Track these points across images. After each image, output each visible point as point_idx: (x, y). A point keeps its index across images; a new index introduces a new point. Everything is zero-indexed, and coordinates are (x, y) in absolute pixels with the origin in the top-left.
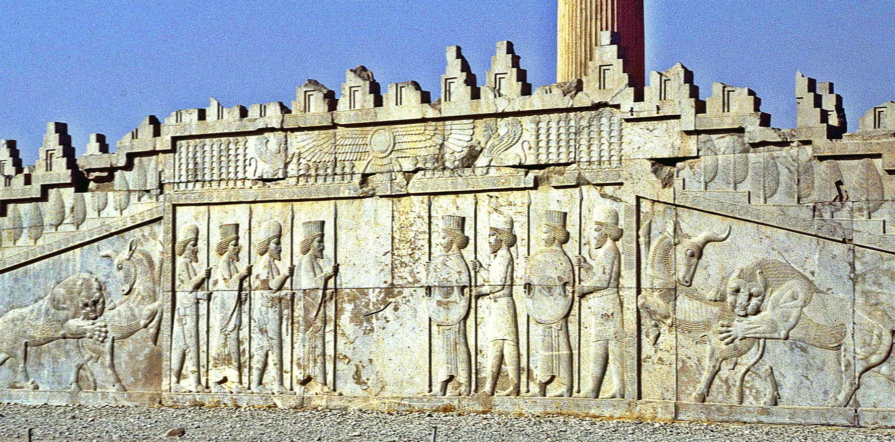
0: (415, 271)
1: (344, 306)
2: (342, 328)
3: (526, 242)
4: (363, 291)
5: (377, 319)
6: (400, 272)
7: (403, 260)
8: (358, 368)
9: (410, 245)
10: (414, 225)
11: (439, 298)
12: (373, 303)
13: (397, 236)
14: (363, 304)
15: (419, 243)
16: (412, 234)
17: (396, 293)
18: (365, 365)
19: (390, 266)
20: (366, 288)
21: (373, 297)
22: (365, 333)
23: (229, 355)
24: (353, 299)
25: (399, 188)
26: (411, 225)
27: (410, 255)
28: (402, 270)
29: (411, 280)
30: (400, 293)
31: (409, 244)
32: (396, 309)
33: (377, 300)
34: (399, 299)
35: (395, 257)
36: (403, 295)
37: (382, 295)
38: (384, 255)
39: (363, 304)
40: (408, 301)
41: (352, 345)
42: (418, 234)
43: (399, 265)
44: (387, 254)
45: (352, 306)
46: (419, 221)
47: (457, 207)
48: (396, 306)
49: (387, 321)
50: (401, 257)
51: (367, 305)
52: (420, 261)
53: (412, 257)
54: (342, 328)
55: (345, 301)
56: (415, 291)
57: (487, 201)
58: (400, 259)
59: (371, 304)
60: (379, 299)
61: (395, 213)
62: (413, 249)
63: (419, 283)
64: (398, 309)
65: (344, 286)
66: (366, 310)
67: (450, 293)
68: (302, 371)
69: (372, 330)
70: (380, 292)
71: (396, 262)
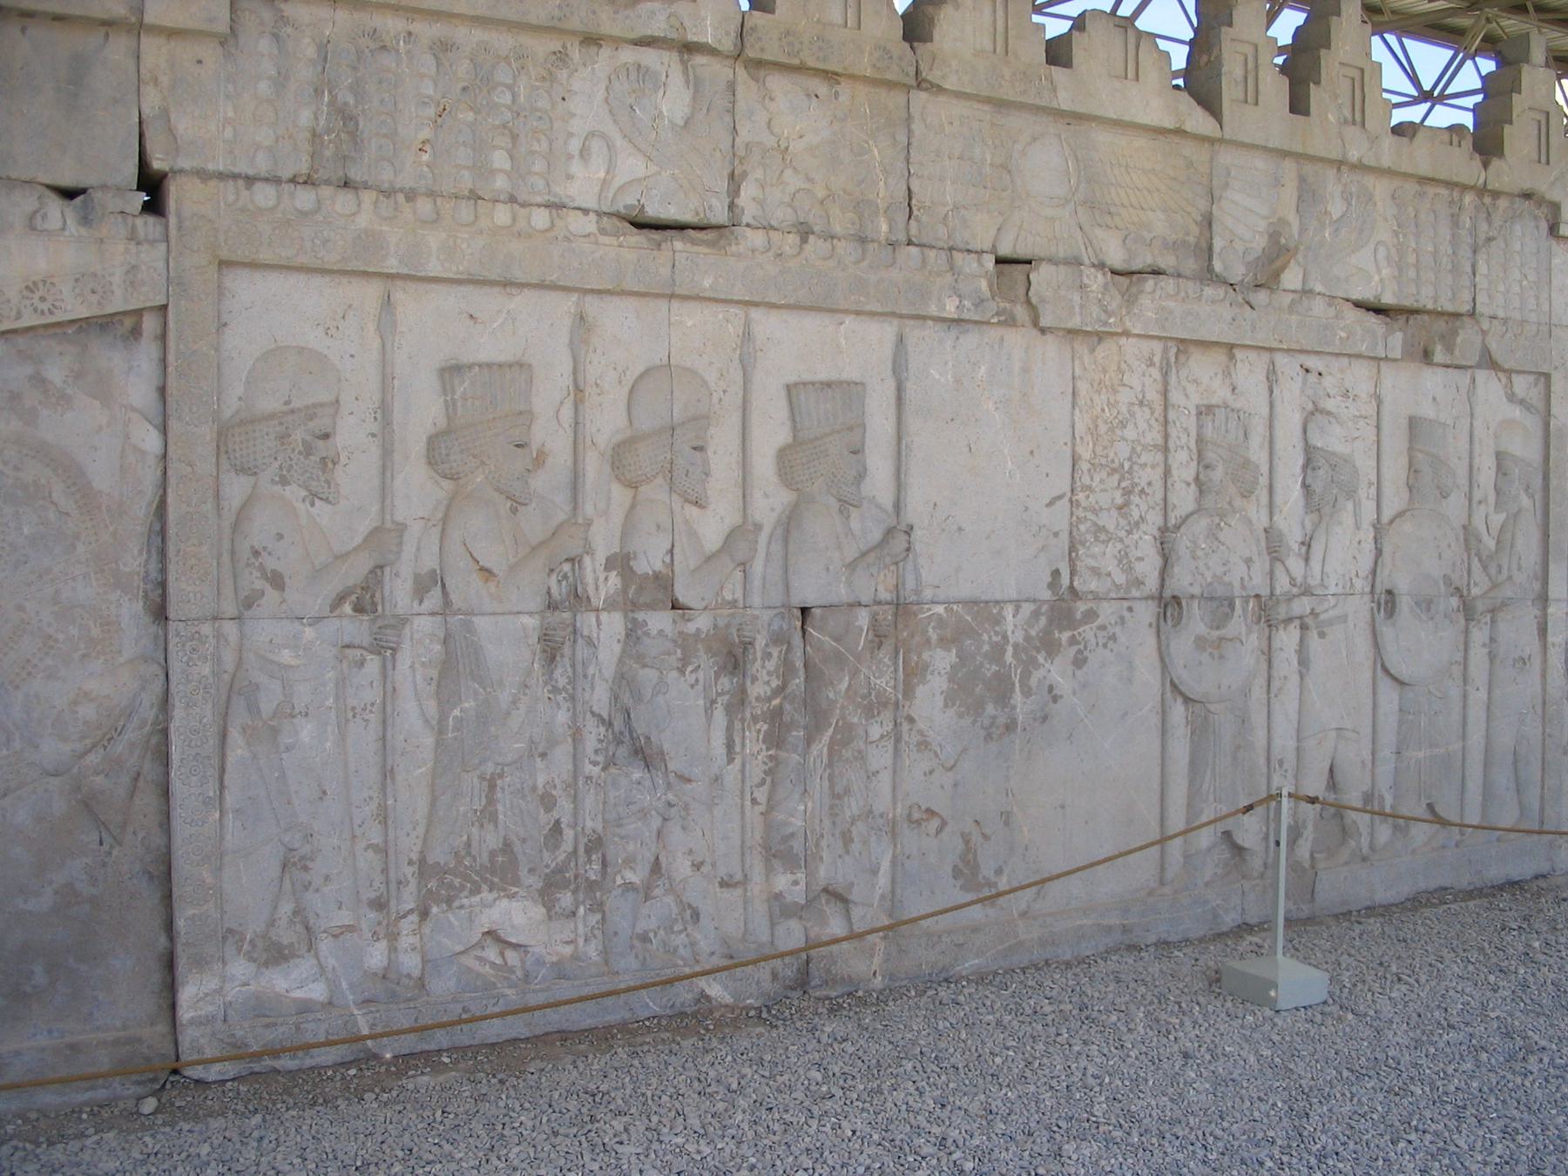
0: (1134, 554)
1: (926, 656)
2: (921, 725)
3: (1373, 490)
4: (985, 609)
5: (1027, 693)
6: (1094, 556)
7: (1101, 523)
8: (967, 842)
9: (1120, 482)
10: (1130, 426)
13: (1085, 452)
14: (986, 648)
15: (1144, 476)
16: (1123, 451)
17: (1078, 616)
18: (988, 831)
19: (1065, 537)
20: (997, 602)
21: (1013, 625)
22: (988, 737)
23: (507, 847)
24: (954, 637)
25: (1103, 317)
26: (1123, 425)
27: (1120, 508)
28: (1097, 549)
29: (1120, 578)
30: (1091, 615)
31: (1117, 476)
32: (1079, 662)
33: (1028, 638)
34: (1087, 631)
35: (1080, 513)
36: (1099, 622)
37: (1043, 621)
38: (1047, 505)
39: (986, 648)
40: (1113, 638)
41: (950, 774)
42: (1139, 449)
43: (1090, 538)
44: (1059, 504)
46: (1142, 415)
48: (1080, 652)
49: (1055, 699)
50: (1095, 512)
51: (998, 651)
52: (1143, 527)
53: (1125, 516)
54: (921, 725)
55: (928, 641)
56: (1130, 609)
57: (1299, 380)
58: (1092, 517)
59: (1010, 650)
60: (1033, 633)
61: (1083, 387)
62: (1127, 492)
64: (1085, 660)
65: (928, 594)
66: (994, 668)
67: (1227, 614)
68: (801, 876)
69: (1010, 727)
70: (1036, 614)
71: (1082, 528)
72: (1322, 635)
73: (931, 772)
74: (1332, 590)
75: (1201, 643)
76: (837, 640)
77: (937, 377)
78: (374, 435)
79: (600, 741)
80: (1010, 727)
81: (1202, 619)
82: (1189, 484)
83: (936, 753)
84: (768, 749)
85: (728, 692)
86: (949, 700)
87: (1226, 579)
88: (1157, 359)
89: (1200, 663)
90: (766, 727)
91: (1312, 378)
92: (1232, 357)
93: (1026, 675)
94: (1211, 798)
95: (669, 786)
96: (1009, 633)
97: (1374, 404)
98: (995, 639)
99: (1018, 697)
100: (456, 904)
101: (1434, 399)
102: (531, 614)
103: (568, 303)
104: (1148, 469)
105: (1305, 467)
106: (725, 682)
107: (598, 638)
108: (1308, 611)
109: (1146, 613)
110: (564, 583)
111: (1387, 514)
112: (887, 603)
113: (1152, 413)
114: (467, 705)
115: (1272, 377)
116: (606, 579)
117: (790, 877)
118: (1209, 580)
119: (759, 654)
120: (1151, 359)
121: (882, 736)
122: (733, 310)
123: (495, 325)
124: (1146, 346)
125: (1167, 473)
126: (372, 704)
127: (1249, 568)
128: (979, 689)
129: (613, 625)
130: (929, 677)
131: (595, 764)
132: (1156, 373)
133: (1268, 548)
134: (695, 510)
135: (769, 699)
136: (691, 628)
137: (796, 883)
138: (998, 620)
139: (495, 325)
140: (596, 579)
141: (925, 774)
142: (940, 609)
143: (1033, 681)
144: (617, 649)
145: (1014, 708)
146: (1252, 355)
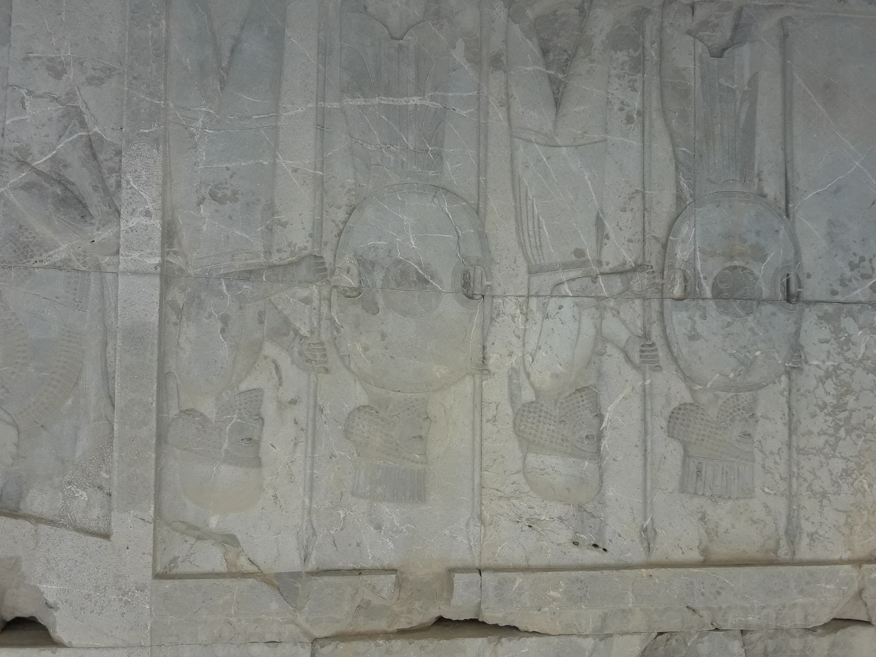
3: (489, 414)
11: (759, 270)
47: (703, 518)
52: (821, 373)
57: (608, 535)
63: (821, 314)
67: (722, 282)
72: (579, 253)
74: (568, 303)
75: (759, 254)
81: (756, 279)
82: (762, 416)
87: (728, 319)
88: (805, 541)
89: (758, 233)
91: (586, 537)
92: (704, 551)
94: (739, 95)
97: (487, 515)
101: (378, 527)
104: (815, 430)
105: (600, 437)
108: (600, 278)
109: (813, 289)
111: (467, 386)
113: (810, 486)
115: (648, 535)
118: (750, 318)
120: (812, 540)
124: (820, 553)
125: (791, 431)
127: (693, 329)
132: (807, 527)
133: (656, 350)
146: (677, 556)
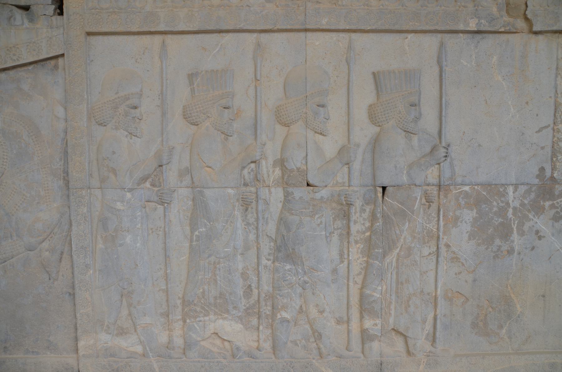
5: (522, 233)
12: (515, 209)
22: (496, 257)
23: (221, 295)
33: (523, 205)
39: (495, 209)
45: (474, 213)
51: (502, 212)
54: (454, 249)
59: (511, 211)
60: (526, 202)
65: (459, 180)
66: (500, 220)
69: (510, 252)
73: (460, 273)
76: (402, 204)
77: (465, 64)
78: (158, 106)
79: (270, 249)
80: (510, 252)
83: (462, 263)
84: (363, 257)
85: (340, 228)
86: (472, 236)
90: (362, 246)
93: (521, 225)
95: (305, 273)
96: (510, 202)
98: (501, 204)
99: (515, 236)
100: (198, 319)
102: (232, 188)
103: (251, 38)
106: (339, 223)
107: (270, 200)
110: (252, 173)
112: (433, 185)
114: (201, 230)
116: (274, 171)
117: (372, 322)
119: (358, 209)
121: (430, 254)
122: (342, 35)
123: (215, 52)
126: (161, 227)
128: (490, 231)
129: (278, 194)
130: (459, 224)
131: (268, 260)
134: (321, 137)
135: (364, 233)
136: (318, 196)
137: (376, 325)
138: (504, 194)
139: (215, 52)
140: (268, 172)
141: (456, 274)
142: (467, 188)
143: (526, 228)
144: (280, 205)
145: (513, 241)
